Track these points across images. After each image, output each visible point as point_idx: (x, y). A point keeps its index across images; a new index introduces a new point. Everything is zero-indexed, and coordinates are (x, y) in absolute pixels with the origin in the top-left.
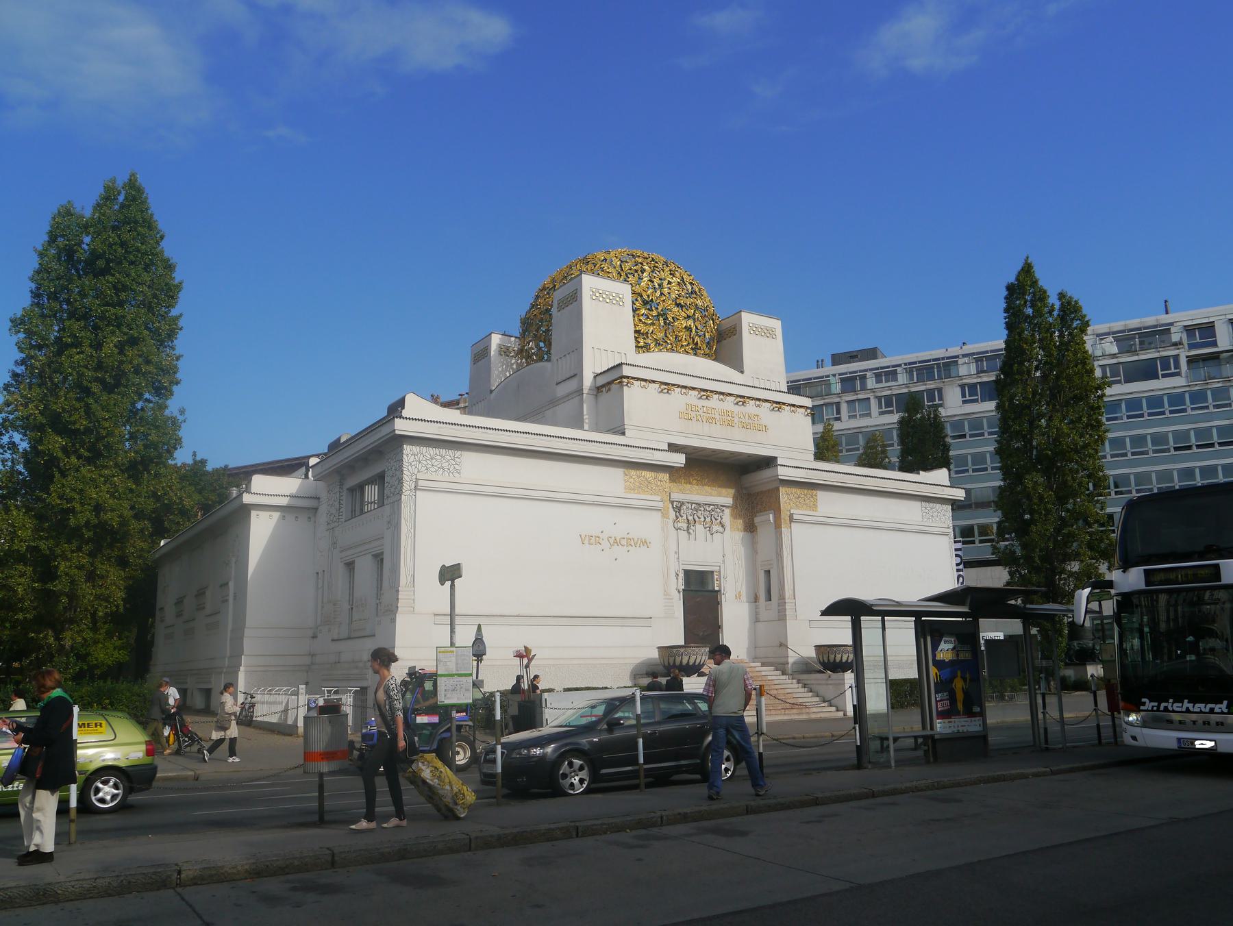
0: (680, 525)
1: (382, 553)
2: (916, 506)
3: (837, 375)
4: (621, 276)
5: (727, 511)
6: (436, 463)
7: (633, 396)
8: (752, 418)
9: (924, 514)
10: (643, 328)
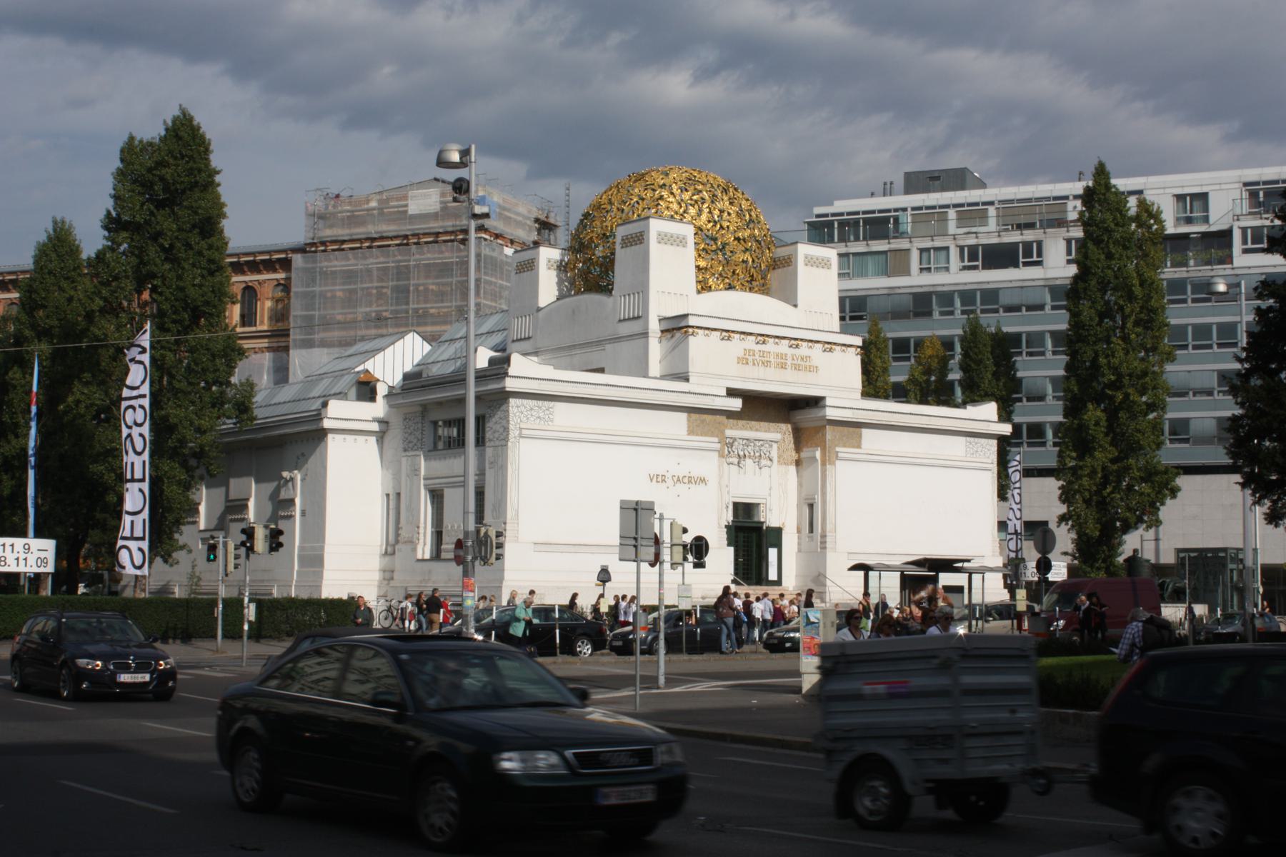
0: (730, 460)
2: (962, 440)
3: (909, 209)
4: (681, 207)
7: (698, 346)
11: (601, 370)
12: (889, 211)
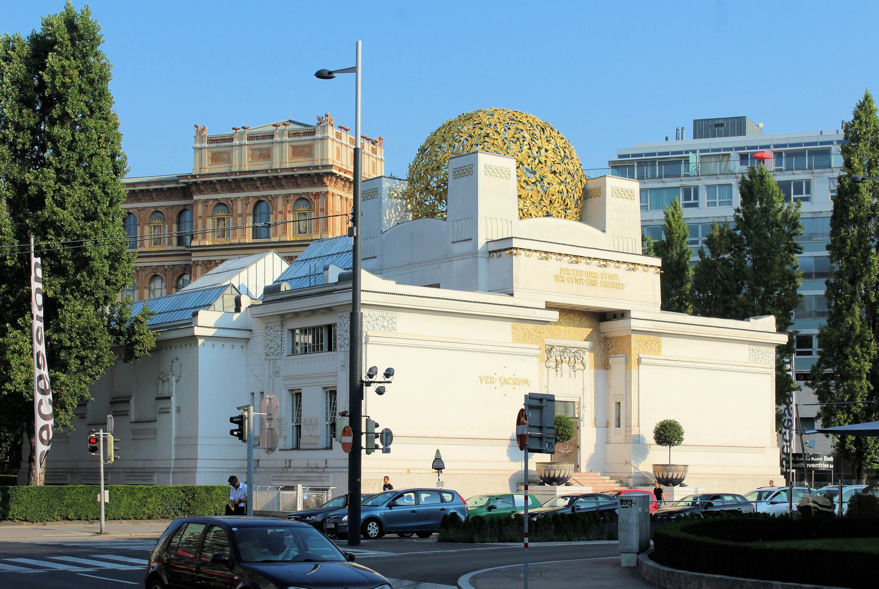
0: (550, 364)
2: (746, 347)
3: (698, 152)
4: (505, 144)
8: (612, 278)
9: (751, 356)
10: (524, 193)
11: (438, 286)
12: (681, 152)
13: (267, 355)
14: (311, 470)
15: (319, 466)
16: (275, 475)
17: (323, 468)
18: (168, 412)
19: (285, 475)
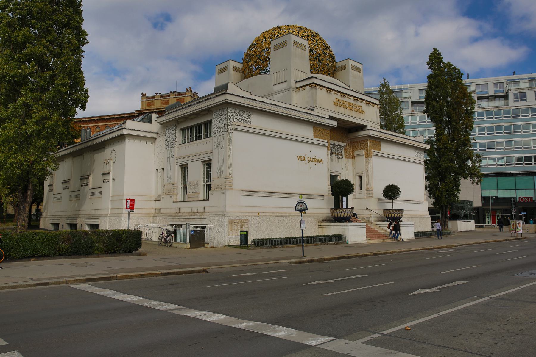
1: (211, 160)
5: (344, 149)
6: (241, 118)
13: (167, 146)
14: (194, 214)
15: (199, 211)
16: (170, 217)
17: (202, 213)
18: (108, 181)
19: (176, 217)
